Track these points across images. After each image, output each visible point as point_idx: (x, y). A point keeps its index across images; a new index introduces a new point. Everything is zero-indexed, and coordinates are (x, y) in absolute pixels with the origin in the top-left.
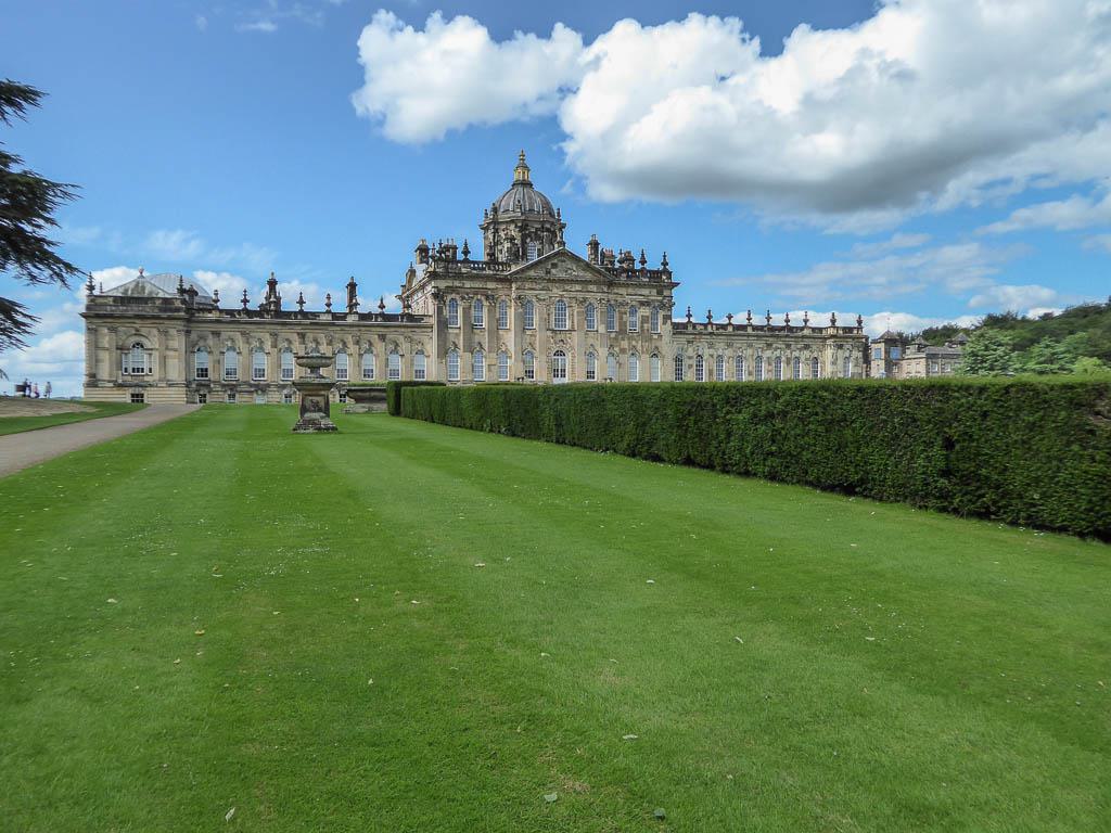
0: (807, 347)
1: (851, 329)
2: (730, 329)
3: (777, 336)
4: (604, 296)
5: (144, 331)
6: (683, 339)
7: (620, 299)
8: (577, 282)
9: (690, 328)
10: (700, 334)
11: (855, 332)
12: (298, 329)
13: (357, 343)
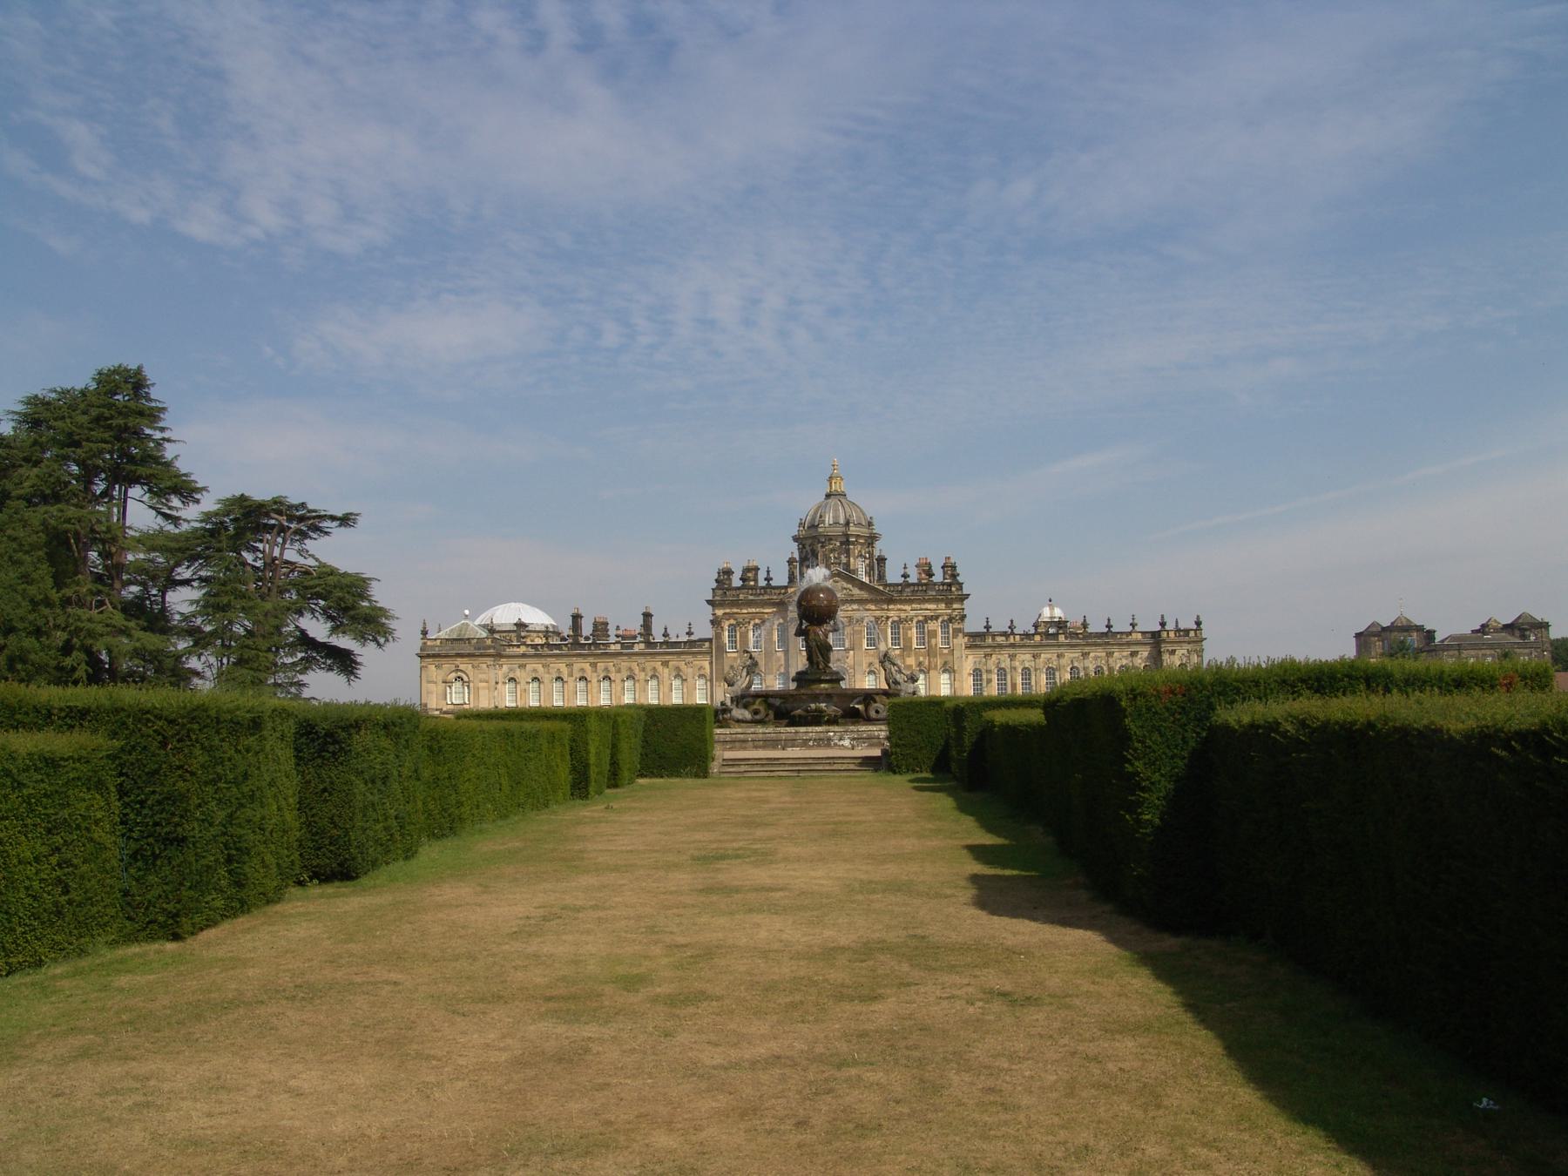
0: (1133, 654)
1: (1187, 631)
2: (1038, 638)
3: (1096, 645)
4: (883, 613)
5: (462, 667)
6: (981, 652)
7: (903, 615)
8: (852, 602)
9: (989, 640)
10: (1000, 646)
11: (1192, 634)
12: (591, 660)
13: (644, 670)
